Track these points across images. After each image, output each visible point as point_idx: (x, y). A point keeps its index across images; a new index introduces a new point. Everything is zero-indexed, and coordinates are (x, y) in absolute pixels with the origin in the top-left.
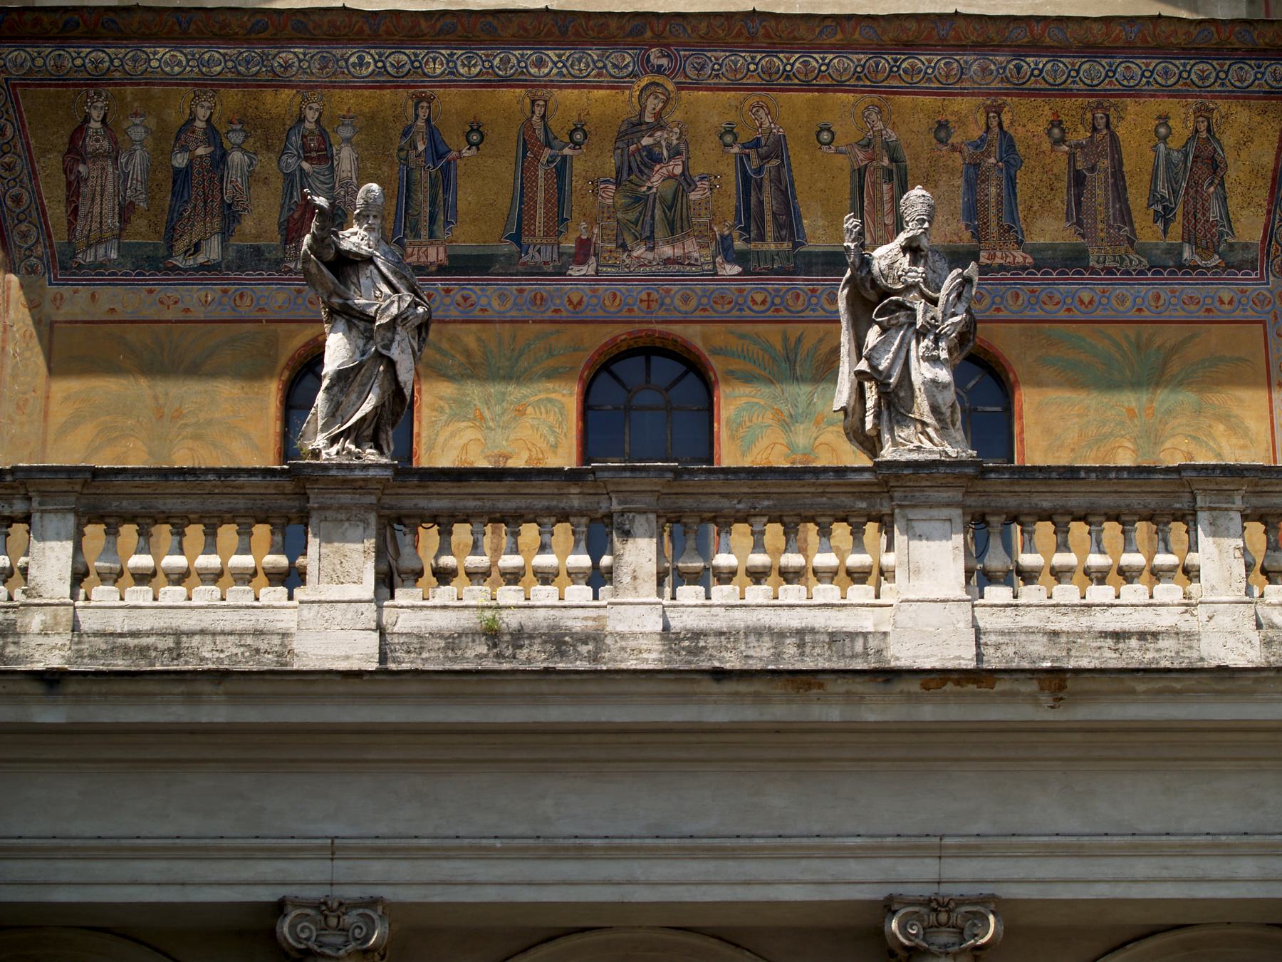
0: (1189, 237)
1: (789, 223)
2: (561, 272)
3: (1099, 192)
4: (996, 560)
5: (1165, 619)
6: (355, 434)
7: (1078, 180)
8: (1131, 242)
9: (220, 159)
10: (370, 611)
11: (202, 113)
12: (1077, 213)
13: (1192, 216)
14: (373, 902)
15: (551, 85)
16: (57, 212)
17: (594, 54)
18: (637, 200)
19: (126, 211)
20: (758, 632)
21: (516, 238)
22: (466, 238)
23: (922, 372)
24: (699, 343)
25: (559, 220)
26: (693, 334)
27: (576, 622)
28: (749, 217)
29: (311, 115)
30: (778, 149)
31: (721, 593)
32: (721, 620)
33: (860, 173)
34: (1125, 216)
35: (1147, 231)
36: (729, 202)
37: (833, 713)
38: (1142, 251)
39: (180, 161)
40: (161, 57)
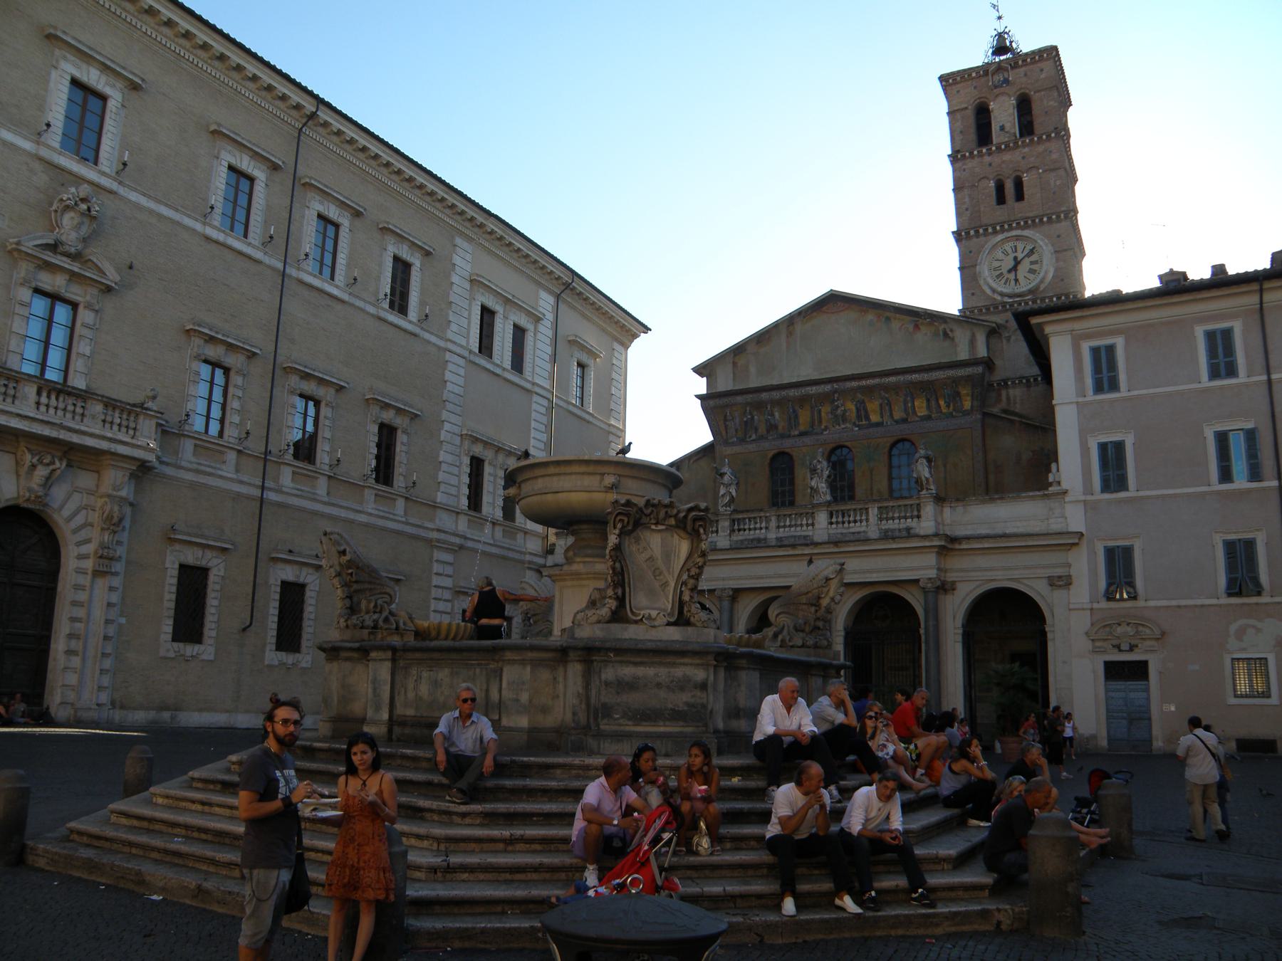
0: (954, 410)
1: (867, 418)
2: (822, 433)
3: (933, 403)
4: (834, 520)
5: (863, 529)
6: (726, 505)
7: (928, 400)
8: (941, 412)
9: (753, 418)
10: (728, 537)
11: (748, 409)
12: (929, 407)
13: (954, 405)
14: (729, 588)
15: (813, 395)
16: (724, 433)
17: (822, 386)
18: (836, 416)
19: (736, 431)
20: (792, 536)
21: (812, 427)
22: (802, 428)
23: (820, 485)
24: (850, 446)
25: (820, 421)
26: (848, 444)
27: (762, 537)
28: (859, 417)
29: (769, 407)
30: (863, 402)
31: (786, 529)
32: (786, 535)
33: (881, 405)
34: (939, 406)
35: (944, 411)
36: (854, 415)
37: (800, 552)
38: (944, 414)
39: (745, 419)
40: (739, 399)
